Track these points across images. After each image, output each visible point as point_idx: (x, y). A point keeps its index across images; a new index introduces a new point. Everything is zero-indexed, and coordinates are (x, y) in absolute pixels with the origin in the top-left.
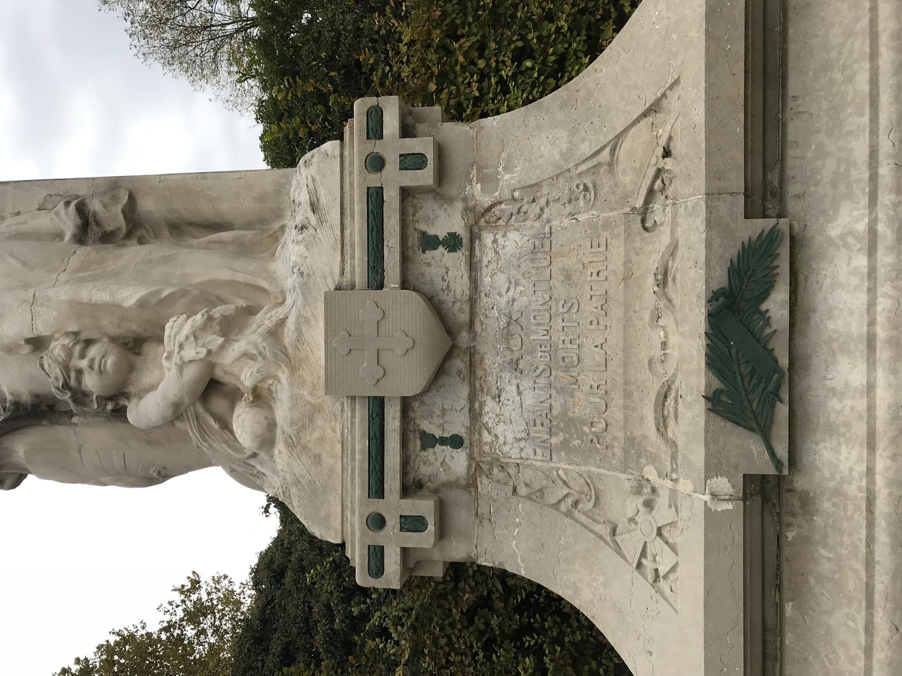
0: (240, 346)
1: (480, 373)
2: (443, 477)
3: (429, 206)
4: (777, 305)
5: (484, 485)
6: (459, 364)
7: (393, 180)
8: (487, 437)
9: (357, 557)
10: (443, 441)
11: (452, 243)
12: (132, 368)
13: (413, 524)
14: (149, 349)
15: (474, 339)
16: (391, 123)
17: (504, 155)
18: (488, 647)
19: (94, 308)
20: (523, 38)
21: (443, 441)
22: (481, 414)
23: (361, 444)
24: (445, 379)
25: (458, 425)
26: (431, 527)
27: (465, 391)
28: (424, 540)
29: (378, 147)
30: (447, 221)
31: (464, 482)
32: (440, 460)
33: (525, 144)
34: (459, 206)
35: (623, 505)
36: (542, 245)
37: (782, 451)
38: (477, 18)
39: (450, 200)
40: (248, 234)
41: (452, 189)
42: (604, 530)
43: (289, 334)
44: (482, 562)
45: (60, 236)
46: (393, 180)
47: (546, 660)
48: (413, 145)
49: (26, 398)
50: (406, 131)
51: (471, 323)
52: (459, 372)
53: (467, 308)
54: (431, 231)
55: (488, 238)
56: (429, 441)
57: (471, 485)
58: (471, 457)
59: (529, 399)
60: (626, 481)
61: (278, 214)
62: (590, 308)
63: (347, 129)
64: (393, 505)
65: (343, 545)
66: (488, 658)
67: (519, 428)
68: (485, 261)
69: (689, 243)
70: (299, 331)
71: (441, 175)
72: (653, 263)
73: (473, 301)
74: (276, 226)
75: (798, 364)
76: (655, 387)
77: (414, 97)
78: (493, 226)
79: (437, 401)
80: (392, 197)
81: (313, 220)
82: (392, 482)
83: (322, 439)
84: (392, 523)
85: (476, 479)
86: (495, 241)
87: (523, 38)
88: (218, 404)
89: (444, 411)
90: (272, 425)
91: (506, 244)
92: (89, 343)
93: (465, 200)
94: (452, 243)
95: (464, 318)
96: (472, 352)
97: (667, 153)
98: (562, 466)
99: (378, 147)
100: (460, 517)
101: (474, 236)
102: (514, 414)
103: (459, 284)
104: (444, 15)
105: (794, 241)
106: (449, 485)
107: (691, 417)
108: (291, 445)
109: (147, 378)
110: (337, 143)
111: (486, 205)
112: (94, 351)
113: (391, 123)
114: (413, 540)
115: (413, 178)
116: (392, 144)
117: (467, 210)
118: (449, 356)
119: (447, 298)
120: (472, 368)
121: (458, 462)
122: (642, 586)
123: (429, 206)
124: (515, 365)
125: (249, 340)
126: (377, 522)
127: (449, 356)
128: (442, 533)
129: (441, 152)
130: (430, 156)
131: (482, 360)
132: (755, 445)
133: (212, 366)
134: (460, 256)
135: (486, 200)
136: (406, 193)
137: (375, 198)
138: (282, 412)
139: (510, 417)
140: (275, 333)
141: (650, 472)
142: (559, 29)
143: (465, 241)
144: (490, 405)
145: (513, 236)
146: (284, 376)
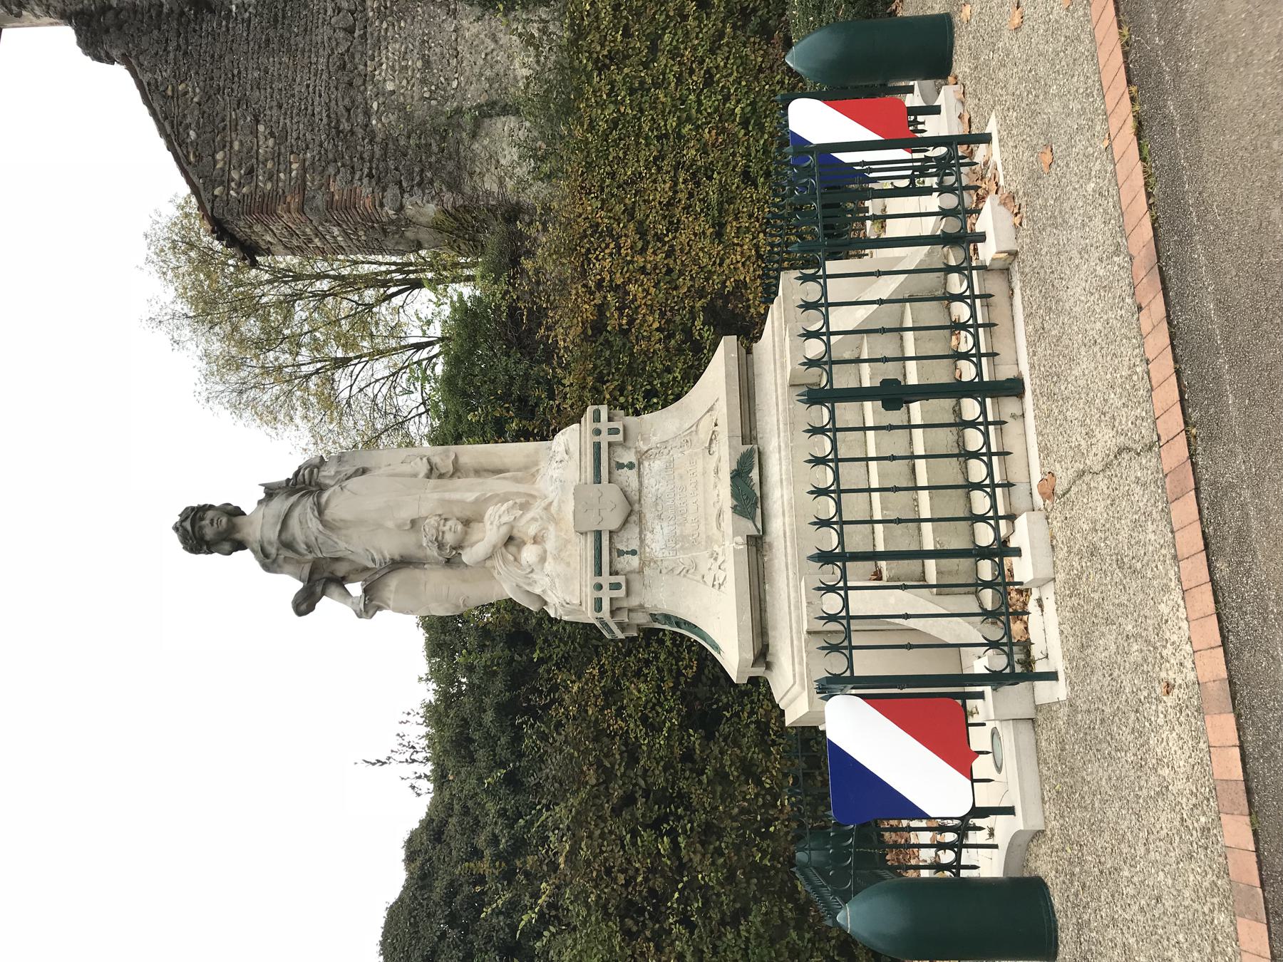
0: (529, 515)
2: (628, 569)
3: (619, 450)
4: (755, 474)
5: (647, 571)
6: (634, 518)
7: (605, 439)
8: (648, 550)
10: (627, 553)
12: (466, 533)
13: (615, 586)
14: (475, 526)
16: (604, 416)
18: (635, 834)
19: (450, 502)
20: (650, 383)
21: (627, 553)
23: (590, 553)
24: (628, 525)
25: (634, 545)
26: (624, 587)
28: (621, 593)
29: (598, 425)
30: (627, 457)
33: (660, 425)
35: (705, 565)
36: (670, 466)
37: (760, 526)
38: (617, 369)
40: (520, 474)
41: (630, 444)
42: (699, 578)
43: (554, 509)
45: (415, 476)
46: (605, 439)
47: (680, 839)
48: (613, 425)
49: (397, 557)
50: (610, 419)
55: (646, 464)
56: (621, 553)
57: (641, 571)
59: (666, 531)
60: (706, 554)
61: (536, 463)
62: (690, 488)
64: (606, 579)
66: (634, 844)
67: (662, 544)
69: (725, 457)
70: (560, 507)
71: (625, 439)
72: (712, 466)
73: (640, 491)
74: (534, 470)
75: (763, 497)
76: (715, 512)
77: (613, 404)
78: (648, 459)
79: (625, 535)
80: (604, 447)
81: (566, 457)
82: (606, 569)
83: (570, 555)
84: (606, 587)
87: (650, 383)
88: (512, 549)
90: (545, 551)
91: (653, 468)
92: (446, 520)
95: (637, 498)
96: (640, 513)
98: (682, 556)
99: (598, 425)
100: (636, 586)
103: (634, 484)
104: (595, 367)
105: (759, 453)
106: (631, 572)
107: (728, 514)
108: (555, 558)
109: (474, 538)
112: (449, 523)
113: (604, 416)
114: (615, 594)
116: (604, 424)
120: (640, 521)
121: (634, 562)
122: (715, 591)
123: (619, 450)
124: (660, 517)
125: (536, 510)
126: (599, 587)
128: (628, 594)
132: (750, 524)
133: (512, 528)
134: (635, 471)
135: (645, 448)
136: (610, 444)
137: (597, 447)
138: (550, 545)
139: (657, 540)
140: (547, 508)
141: (716, 548)
142: (674, 378)
144: (649, 535)
145: (657, 462)
146: (552, 528)
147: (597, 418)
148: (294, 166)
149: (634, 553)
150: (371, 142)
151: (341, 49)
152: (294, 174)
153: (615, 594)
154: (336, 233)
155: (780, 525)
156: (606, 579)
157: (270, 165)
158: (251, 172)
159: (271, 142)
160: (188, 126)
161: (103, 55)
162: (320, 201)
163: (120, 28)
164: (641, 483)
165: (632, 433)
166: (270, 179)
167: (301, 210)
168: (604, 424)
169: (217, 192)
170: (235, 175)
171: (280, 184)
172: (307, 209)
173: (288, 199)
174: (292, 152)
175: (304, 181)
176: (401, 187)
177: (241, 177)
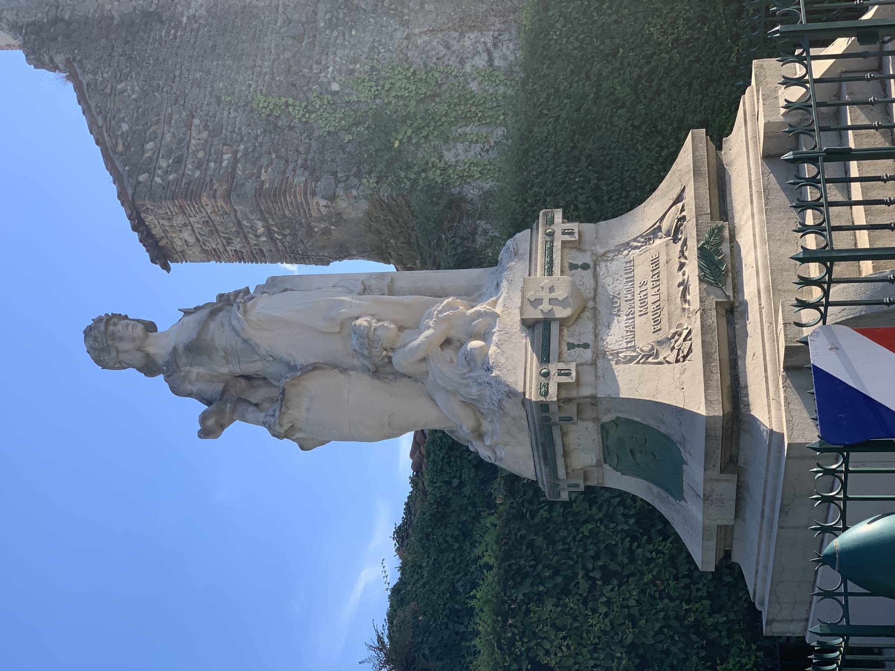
1: (598, 317)
4: (725, 248)
6: (588, 314)
10: (579, 346)
11: (585, 267)
21: (579, 346)
24: (580, 320)
25: (588, 338)
27: (591, 325)
34: (589, 253)
39: (584, 251)
51: (594, 298)
52: (588, 317)
53: (592, 292)
54: (574, 263)
55: (603, 265)
57: (594, 363)
63: (535, 226)
68: (601, 273)
73: (596, 290)
82: (554, 354)
89: (580, 334)
94: (585, 267)
95: (592, 295)
96: (595, 309)
115: (567, 238)
117: (593, 254)
121: (588, 355)
127: (583, 310)
134: (589, 272)
135: (601, 251)
143: (592, 266)
147: (551, 222)
148: (226, 157)
149: (586, 346)
150: (309, 137)
151: (287, 55)
152: (224, 164)
153: (564, 379)
154: (261, 230)
155: (753, 284)
156: (553, 368)
157: (201, 154)
158: (179, 161)
159: (205, 134)
160: (122, 120)
161: (47, 59)
162: (250, 186)
163: (68, 36)
166: (198, 167)
167: (227, 197)
169: (142, 178)
170: (163, 163)
171: (209, 173)
172: (233, 196)
173: (215, 187)
174: (225, 144)
175: (234, 170)
176: (336, 178)
177: (169, 166)
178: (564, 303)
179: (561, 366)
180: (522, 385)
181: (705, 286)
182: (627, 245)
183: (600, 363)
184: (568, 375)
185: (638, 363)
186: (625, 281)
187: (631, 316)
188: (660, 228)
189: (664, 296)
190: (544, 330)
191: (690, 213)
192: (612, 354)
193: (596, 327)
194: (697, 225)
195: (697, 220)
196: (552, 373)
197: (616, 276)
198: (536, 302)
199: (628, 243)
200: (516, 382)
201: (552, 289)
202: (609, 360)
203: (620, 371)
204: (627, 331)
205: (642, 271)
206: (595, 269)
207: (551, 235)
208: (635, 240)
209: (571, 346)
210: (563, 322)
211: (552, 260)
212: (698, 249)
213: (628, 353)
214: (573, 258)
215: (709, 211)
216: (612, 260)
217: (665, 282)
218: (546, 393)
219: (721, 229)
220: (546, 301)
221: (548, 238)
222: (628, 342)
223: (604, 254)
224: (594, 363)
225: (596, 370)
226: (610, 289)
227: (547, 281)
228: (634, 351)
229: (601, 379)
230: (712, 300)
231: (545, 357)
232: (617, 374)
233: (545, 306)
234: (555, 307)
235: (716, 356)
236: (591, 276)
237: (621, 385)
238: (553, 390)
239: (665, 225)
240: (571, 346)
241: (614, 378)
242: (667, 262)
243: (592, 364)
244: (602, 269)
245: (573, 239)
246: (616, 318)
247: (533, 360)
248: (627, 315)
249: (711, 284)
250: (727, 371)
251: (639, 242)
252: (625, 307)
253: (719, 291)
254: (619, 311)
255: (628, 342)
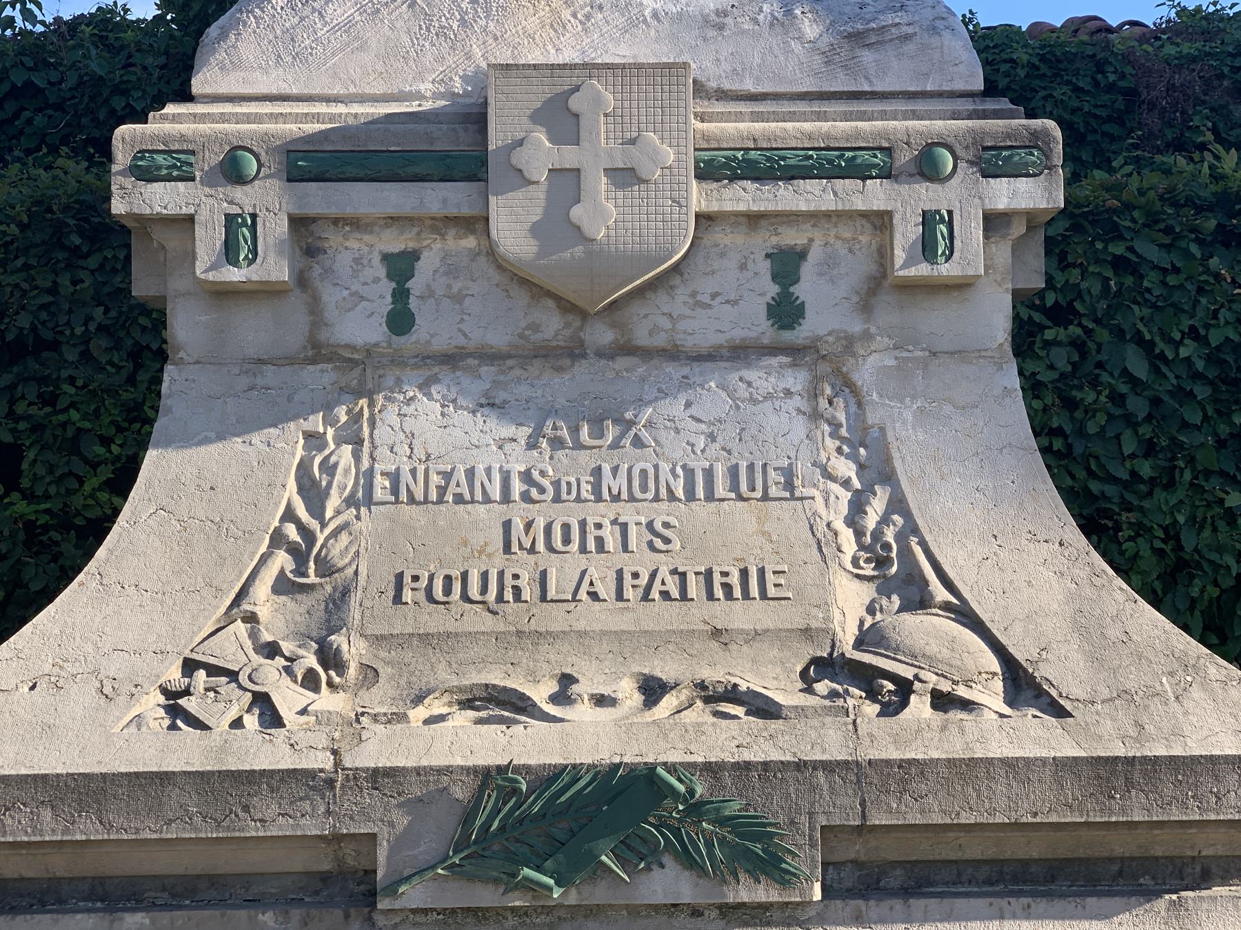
1: (535, 367)
2: (331, 296)
6: (552, 325)
9: (171, 123)
10: (401, 295)
11: (786, 311)
15: (600, 354)
17: (948, 409)
21: (401, 295)
22: (454, 368)
24: (521, 297)
25: (434, 328)
27: (498, 339)
31: (323, 336)
32: (364, 291)
34: (856, 327)
44: (170, 371)
48: (971, 232)
50: (994, 222)
51: (628, 349)
52: (535, 327)
53: (660, 341)
54: (807, 270)
55: (796, 380)
57: (318, 351)
58: (369, 351)
63: (1004, 104)
65: (186, 96)
68: (751, 375)
73: (673, 354)
77: (1062, 236)
82: (321, 198)
85: (329, 360)
86: (788, 393)
89: (458, 298)
93: (867, 336)
94: (786, 311)
95: (642, 338)
96: (576, 351)
97: (942, 701)
100: (254, 331)
101: (795, 352)
102: (458, 433)
106: (315, 309)
107: (473, 745)
110: (979, 85)
111: (856, 377)
115: (907, 232)
117: (849, 343)
118: (567, 307)
119: (677, 303)
121: (361, 326)
127: (567, 307)
129: (960, 287)
130: (946, 269)
131: (559, 370)
134: (759, 326)
136: (881, 221)
143: (788, 336)
147: (993, 162)
153: (208, 240)
156: (269, 201)
164: (709, 357)
165: (937, 320)
168: (967, 198)
178: (557, 225)
179: (274, 228)
180: (223, 90)
181: (461, 792)
182: (879, 471)
183: (321, 376)
184: (230, 253)
185: (289, 515)
186: (699, 465)
187: (517, 487)
188: (918, 601)
189: (554, 618)
190: (444, 156)
191: (919, 732)
192: (356, 418)
193: (490, 356)
194: (800, 766)
195: (828, 767)
196: (238, 193)
197: (728, 434)
198: (561, 117)
199: (888, 477)
200: (237, 65)
201: (625, 177)
202: (328, 408)
203: (286, 444)
204: (447, 476)
205: (736, 532)
206: (774, 350)
207: (926, 168)
208: (898, 504)
209: (400, 267)
210: (478, 223)
211: (792, 174)
212: (651, 768)
213: (344, 481)
214: (830, 263)
215: (878, 819)
216: (815, 416)
217: (623, 622)
218: (144, 173)
219: (771, 866)
220: (569, 156)
221: (904, 157)
222: (395, 478)
223: (847, 386)
224: (318, 351)
225: (291, 361)
226: (674, 407)
227: (669, 154)
228: (350, 501)
229: (244, 381)
230: (384, 823)
231: (311, 162)
232: (256, 438)
233: (542, 154)
234: (539, 194)
235: (86, 829)
236: (738, 334)
237: (215, 449)
238: (161, 198)
239: (930, 631)
240: (400, 267)
241: (244, 426)
242: (716, 633)
243: (315, 344)
244: (765, 378)
245: (900, 256)
246: (524, 433)
247: (296, 124)
248: (526, 477)
249: (467, 819)
250: (60, 866)
251: (885, 520)
252: (572, 467)
253: (426, 849)
254: (557, 443)
255: (395, 478)
